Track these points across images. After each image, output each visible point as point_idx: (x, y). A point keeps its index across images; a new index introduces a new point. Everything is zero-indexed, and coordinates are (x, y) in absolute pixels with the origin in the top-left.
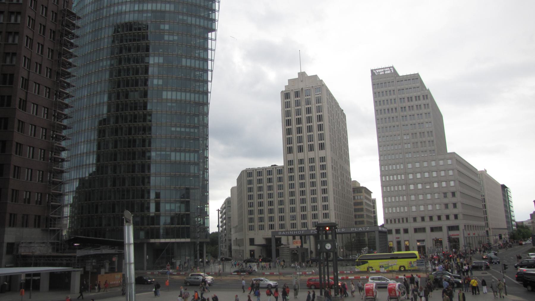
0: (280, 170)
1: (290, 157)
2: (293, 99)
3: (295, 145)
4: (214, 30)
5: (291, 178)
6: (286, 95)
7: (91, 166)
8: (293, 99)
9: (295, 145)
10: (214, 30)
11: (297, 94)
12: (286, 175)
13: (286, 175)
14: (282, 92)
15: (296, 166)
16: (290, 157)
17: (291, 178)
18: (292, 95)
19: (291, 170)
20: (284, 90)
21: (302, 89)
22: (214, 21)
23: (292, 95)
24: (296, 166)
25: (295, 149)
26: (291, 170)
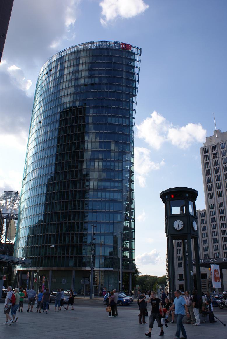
0: (203, 213)
1: (212, 201)
2: (210, 153)
3: (215, 191)
4: (135, 95)
5: (213, 220)
6: (205, 150)
7: (40, 215)
8: (210, 153)
9: (215, 191)
10: (135, 95)
11: (214, 148)
12: (208, 218)
13: (208, 218)
14: (202, 148)
15: (217, 209)
16: (212, 201)
17: (213, 220)
18: (210, 150)
19: (213, 213)
20: (203, 146)
21: (218, 143)
22: (134, 88)
23: (210, 150)
24: (217, 209)
25: (215, 195)
26: (213, 213)
